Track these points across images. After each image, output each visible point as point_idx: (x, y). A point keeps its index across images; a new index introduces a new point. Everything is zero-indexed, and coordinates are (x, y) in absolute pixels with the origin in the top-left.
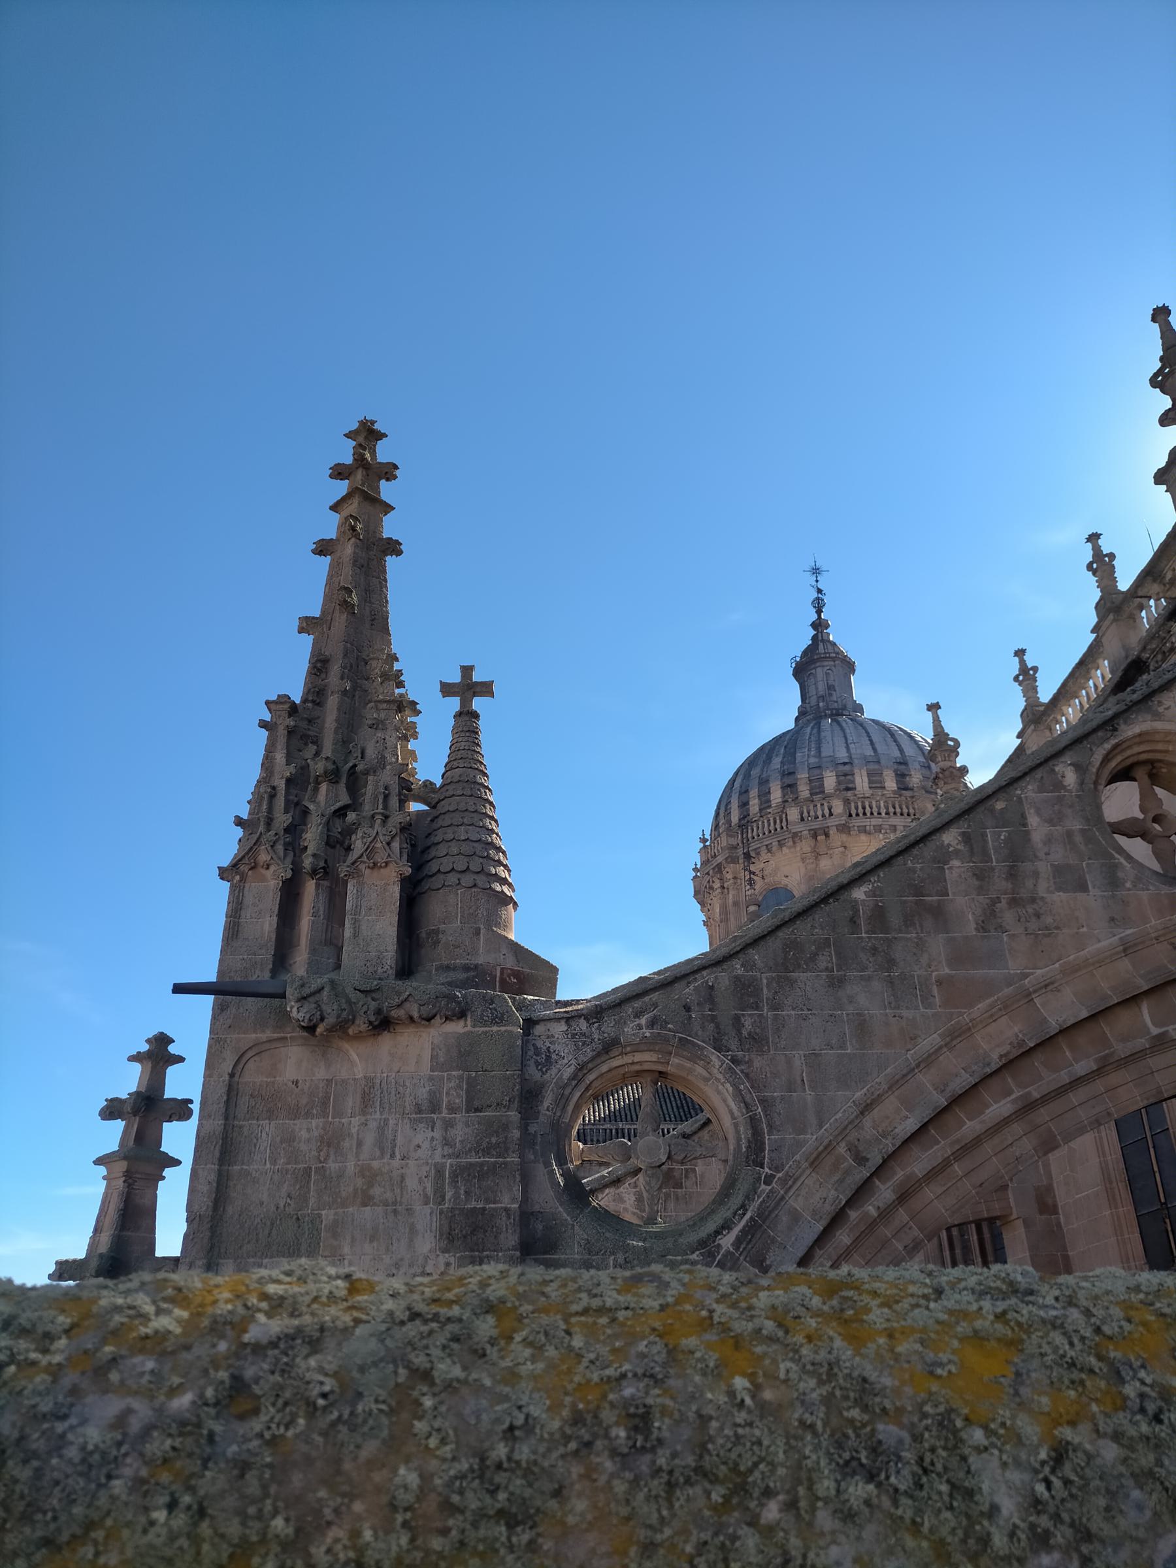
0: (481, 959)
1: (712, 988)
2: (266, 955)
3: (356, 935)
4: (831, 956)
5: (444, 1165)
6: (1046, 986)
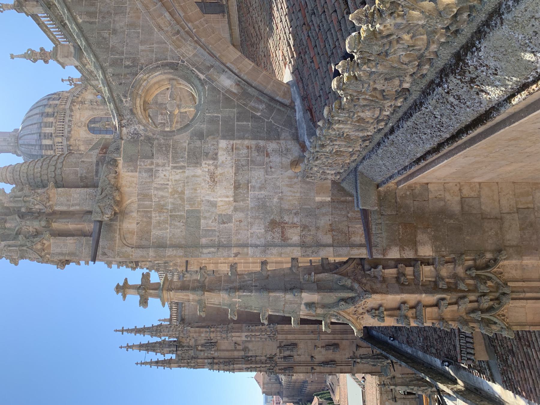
0: (94, 160)
1: (113, 75)
2: (84, 239)
4: (104, 33)
5: (172, 166)
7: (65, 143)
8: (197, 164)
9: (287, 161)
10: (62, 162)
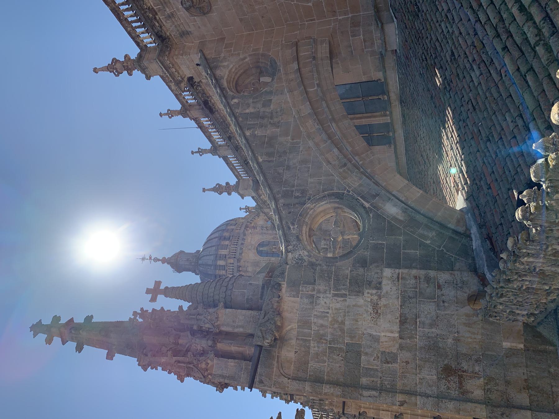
0: (260, 283)
1: (284, 204)
2: (244, 363)
3: (242, 327)
4: (279, 169)
5: (333, 294)
6: (298, 112)
7: (236, 264)
8: (359, 293)
9: (463, 295)
10: (233, 284)
